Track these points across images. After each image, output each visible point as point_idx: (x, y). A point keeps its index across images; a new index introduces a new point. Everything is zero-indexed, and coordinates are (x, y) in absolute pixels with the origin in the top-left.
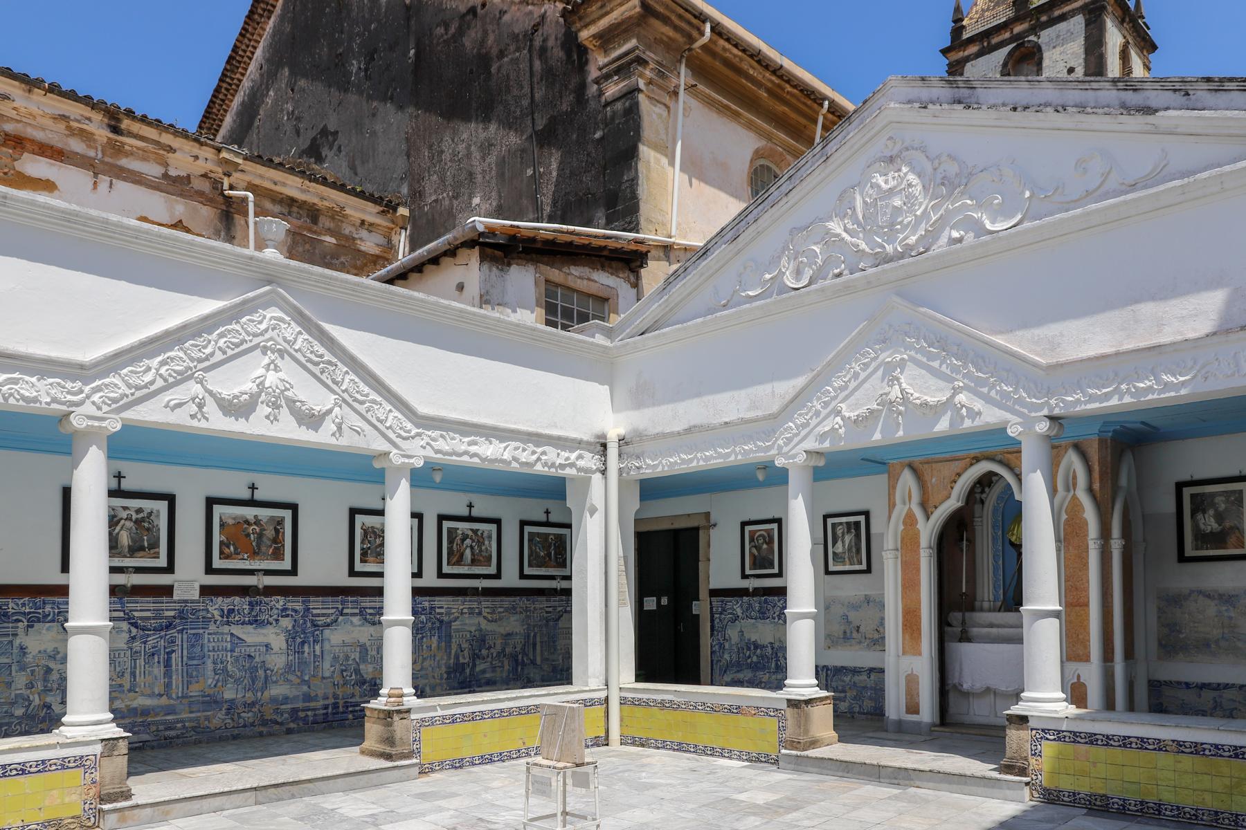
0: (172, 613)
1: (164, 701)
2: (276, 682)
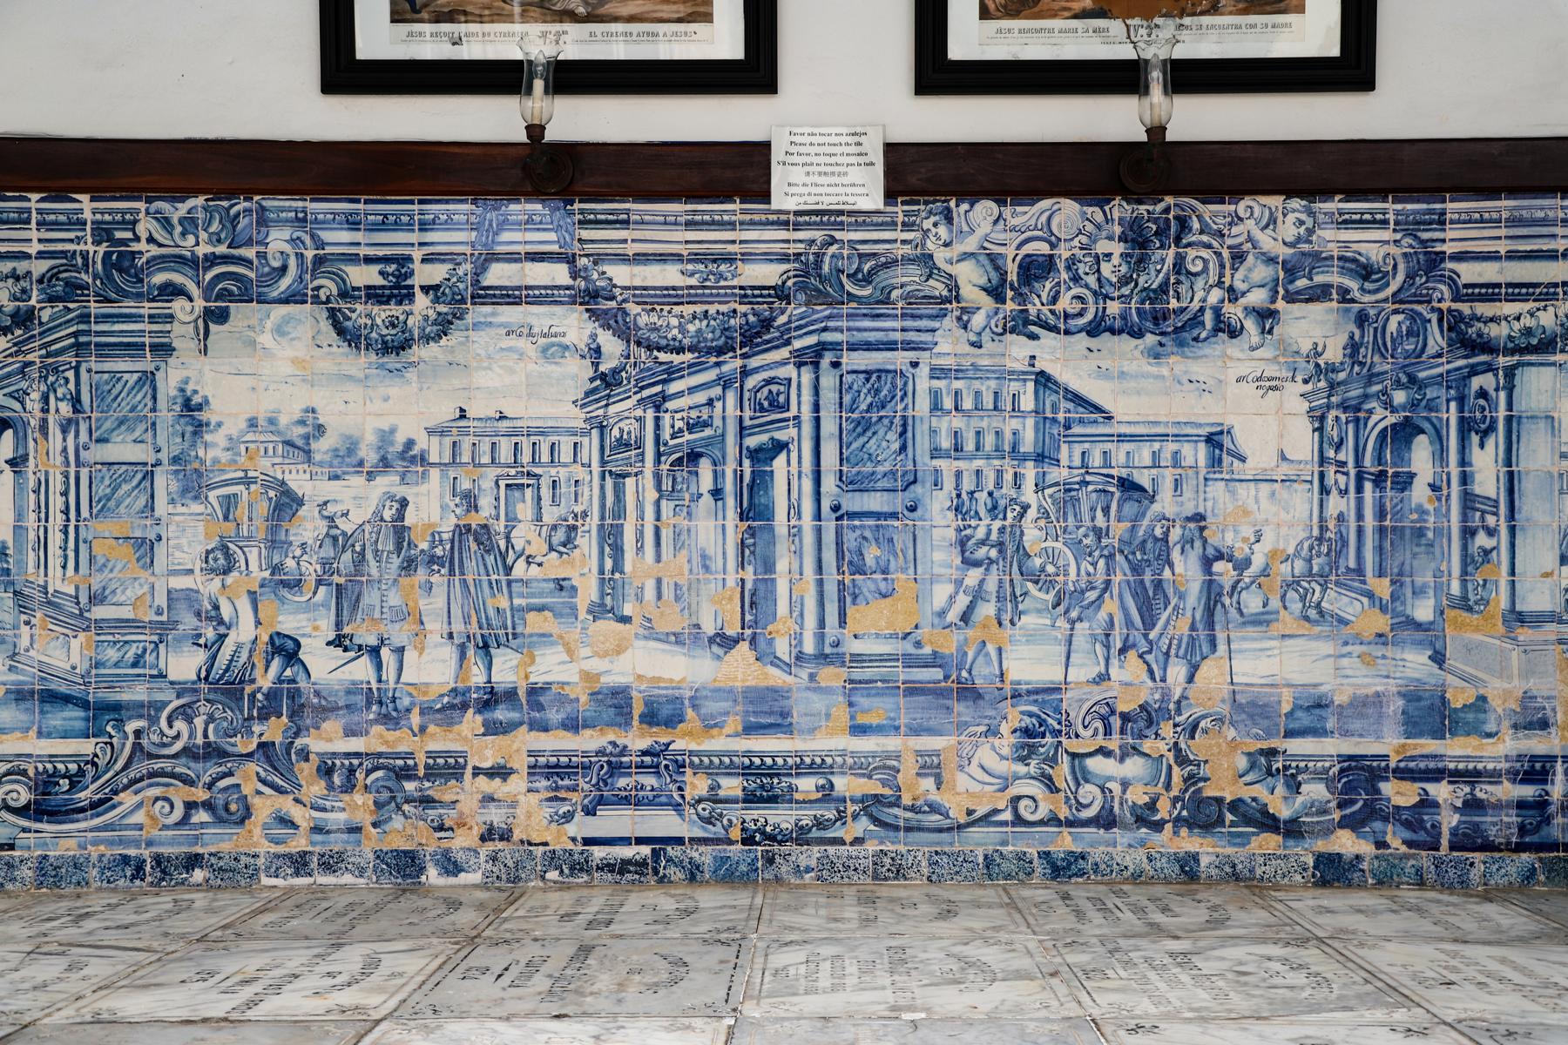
0: (767, 274)
1: (740, 668)
2: (1261, 621)
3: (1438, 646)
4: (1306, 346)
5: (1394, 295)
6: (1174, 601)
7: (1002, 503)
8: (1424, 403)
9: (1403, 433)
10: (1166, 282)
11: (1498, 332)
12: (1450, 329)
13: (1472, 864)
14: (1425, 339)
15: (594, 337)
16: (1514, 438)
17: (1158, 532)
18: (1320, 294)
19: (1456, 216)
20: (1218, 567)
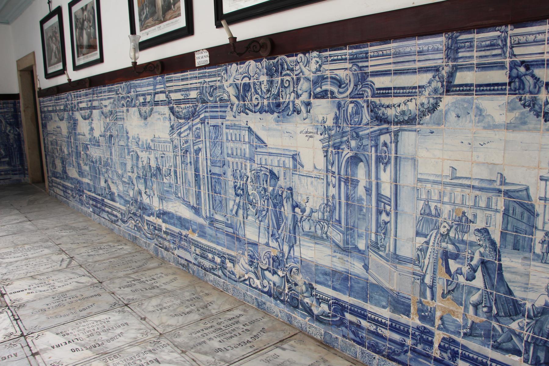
3: (366, 262)
4: (320, 119)
5: (350, 94)
6: (285, 220)
7: (243, 175)
8: (362, 147)
9: (355, 160)
10: (278, 92)
11: (391, 113)
12: (372, 111)
13: (374, 358)
14: (362, 116)
15: (170, 115)
16: (398, 168)
17: (280, 192)
18: (324, 95)
19: (372, 54)
20: (297, 210)
